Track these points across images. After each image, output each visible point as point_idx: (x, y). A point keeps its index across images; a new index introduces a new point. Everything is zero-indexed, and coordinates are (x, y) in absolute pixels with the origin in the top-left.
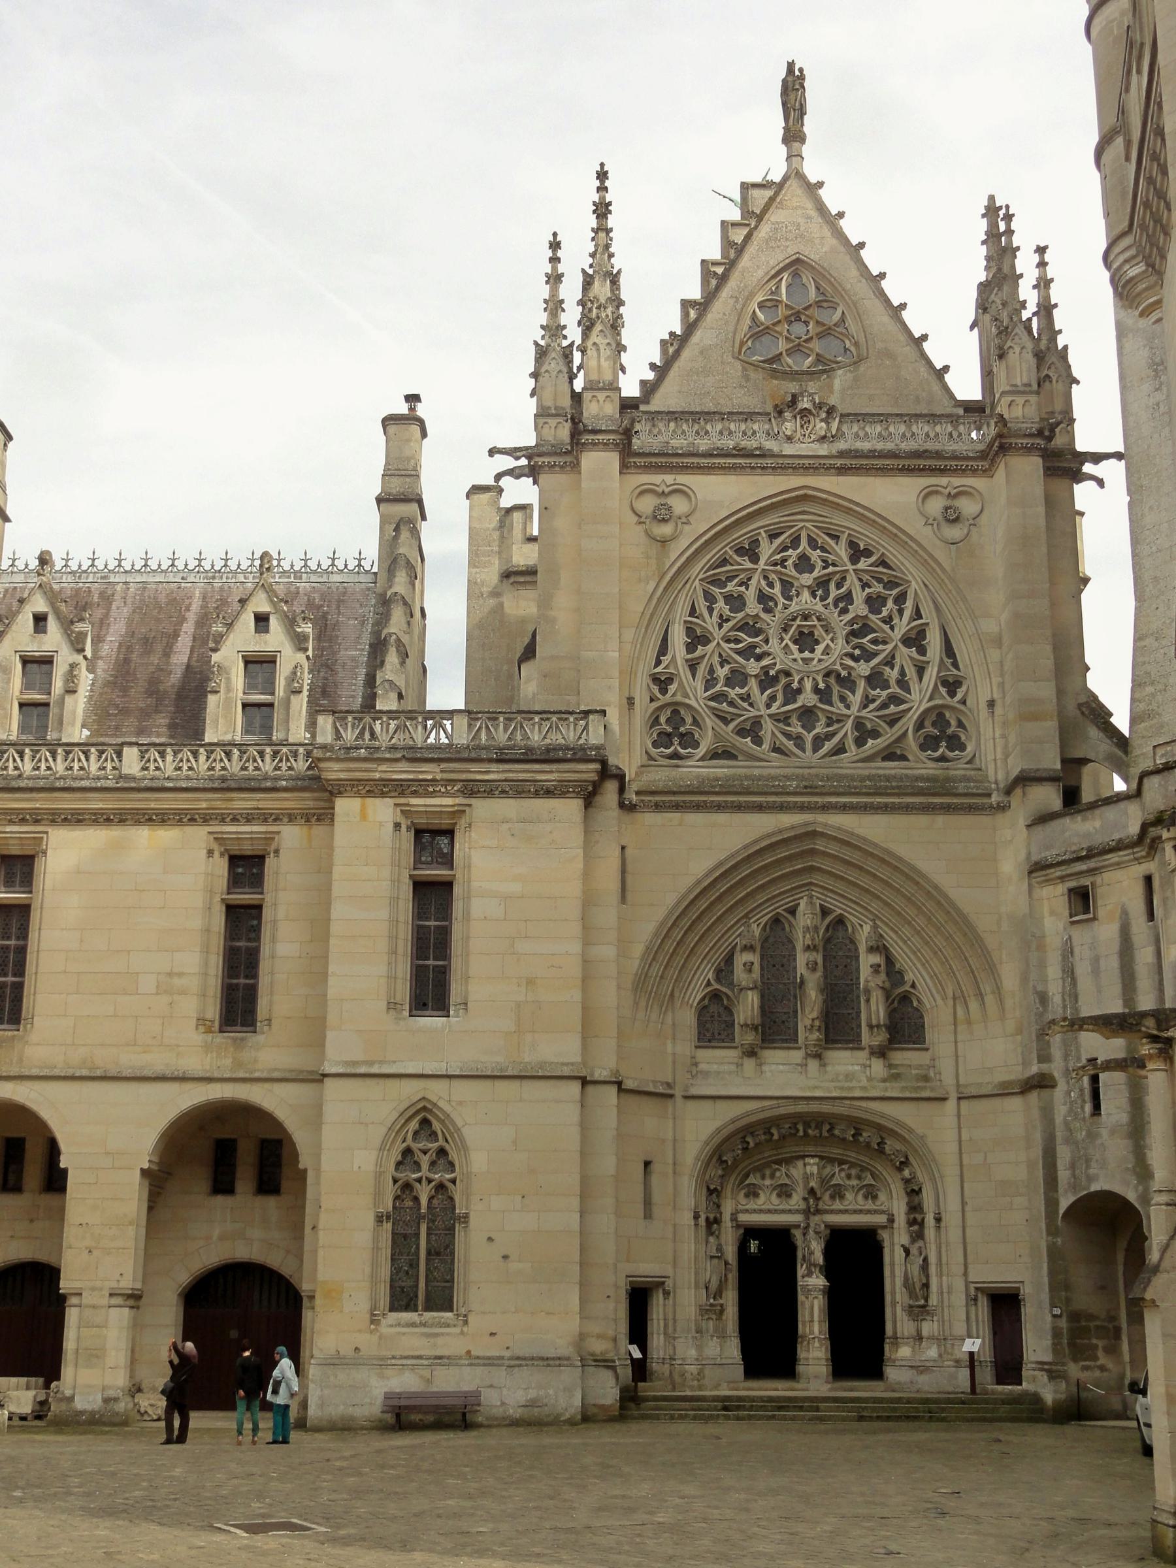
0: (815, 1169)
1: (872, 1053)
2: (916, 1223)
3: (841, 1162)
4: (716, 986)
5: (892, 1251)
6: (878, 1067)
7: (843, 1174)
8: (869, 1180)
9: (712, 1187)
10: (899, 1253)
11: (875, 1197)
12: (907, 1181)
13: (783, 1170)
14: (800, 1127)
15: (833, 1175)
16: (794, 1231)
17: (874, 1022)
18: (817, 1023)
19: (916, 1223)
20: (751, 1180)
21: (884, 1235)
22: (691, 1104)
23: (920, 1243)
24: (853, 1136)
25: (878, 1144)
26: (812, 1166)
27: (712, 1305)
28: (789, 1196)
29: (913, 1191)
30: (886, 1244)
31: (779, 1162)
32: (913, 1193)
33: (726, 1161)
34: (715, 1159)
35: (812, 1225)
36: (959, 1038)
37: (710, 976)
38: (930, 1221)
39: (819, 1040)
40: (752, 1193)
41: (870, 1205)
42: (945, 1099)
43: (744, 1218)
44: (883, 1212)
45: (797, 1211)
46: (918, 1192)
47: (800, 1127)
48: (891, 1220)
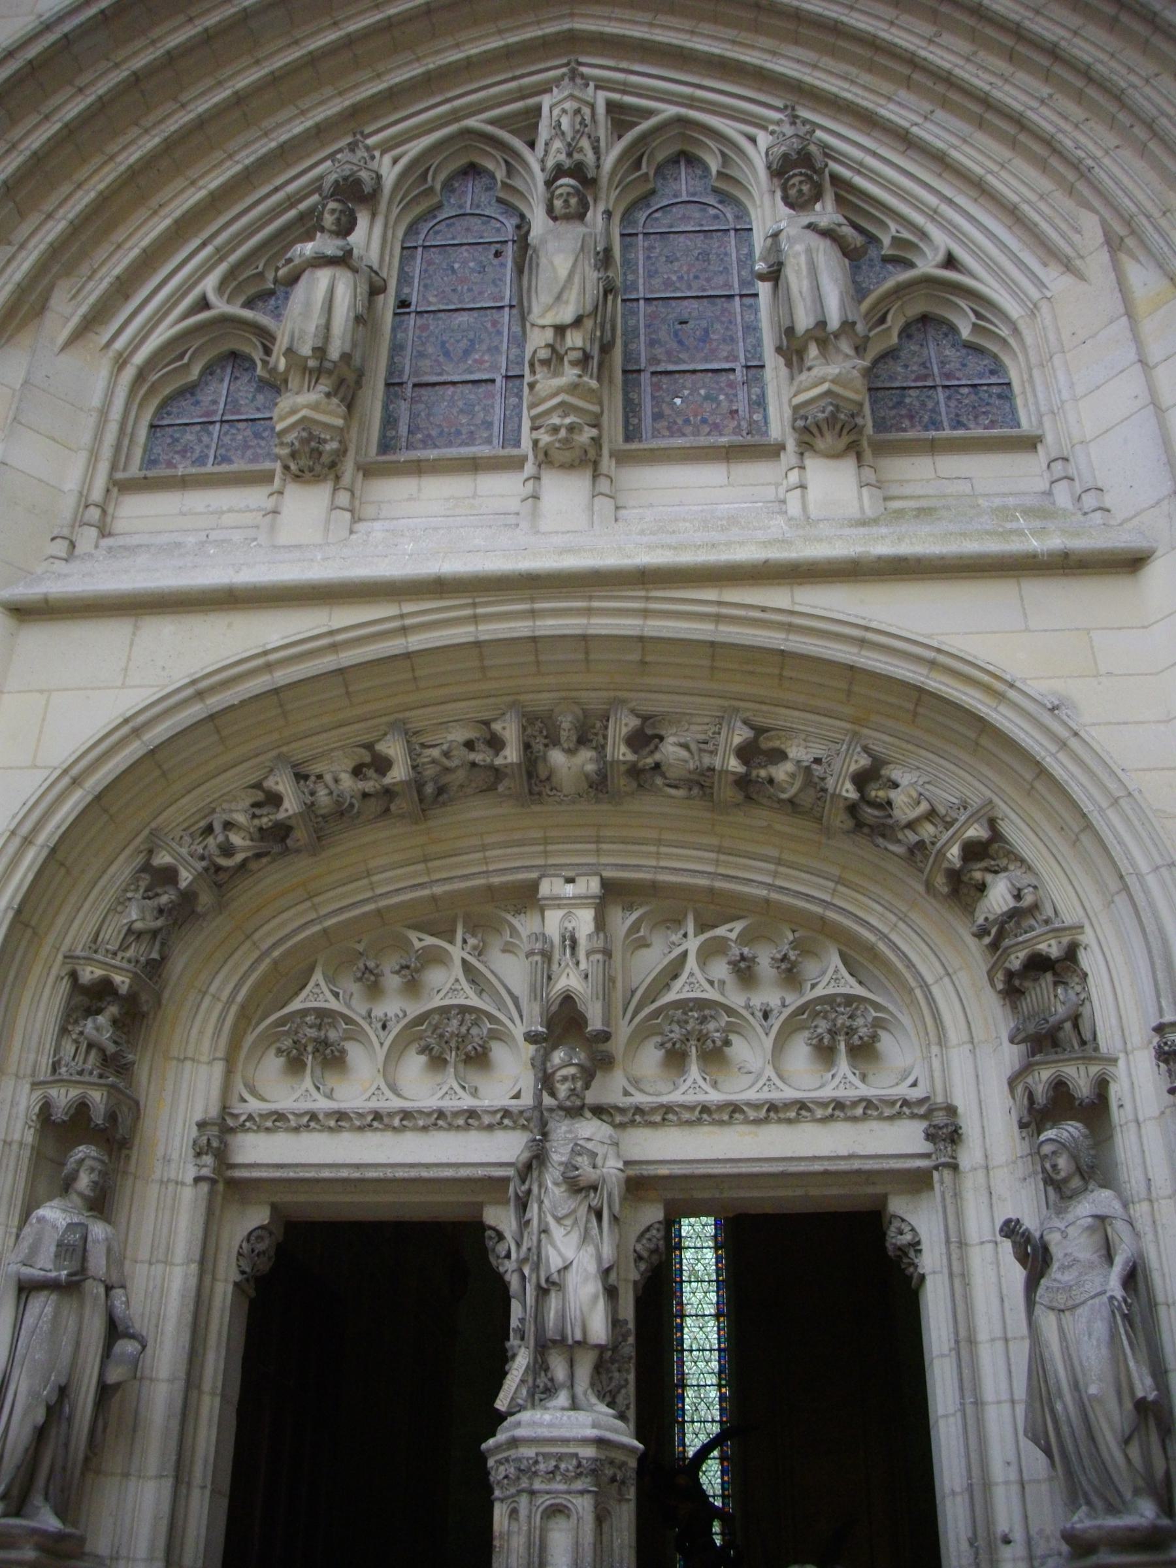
0: (584, 922)
1: (806, 446)
3: (711, 907)
4: (220, 306)
5: (960, 1276)
6: (832, 484)
7: (720, 969)
8: (829, 976)
9: (89, 974)
10: (997, 1273)
11: (864, 1052)
12: (997, 935)
13: (457, 952)
14: (509, 730)
15: (674, 971)
17: (804, 321)
18: (574, 339)
20: (318, 994)
21: (921, 1222)
23: (1098, 1200)
24: (746, 753)
25: (861, 780)
26: (568, 910)
28: (479, 1059)
29: (1038, 964)
31: (440, 918)
32: (1037, 975)
33: (168, 876)
34: (122, 869)
35: (559, 1155)
36: (1155, 352)
37: (209, 284)
39: (573, 388)
40: (318, 1049)
41: (843, 1081)
42: (1131, 563)
43: (258, 1151)
44: (904, 1109)
45: (506, 1118)
46: (1062, 966)
47: (509, 730)
48: (946, 1132)
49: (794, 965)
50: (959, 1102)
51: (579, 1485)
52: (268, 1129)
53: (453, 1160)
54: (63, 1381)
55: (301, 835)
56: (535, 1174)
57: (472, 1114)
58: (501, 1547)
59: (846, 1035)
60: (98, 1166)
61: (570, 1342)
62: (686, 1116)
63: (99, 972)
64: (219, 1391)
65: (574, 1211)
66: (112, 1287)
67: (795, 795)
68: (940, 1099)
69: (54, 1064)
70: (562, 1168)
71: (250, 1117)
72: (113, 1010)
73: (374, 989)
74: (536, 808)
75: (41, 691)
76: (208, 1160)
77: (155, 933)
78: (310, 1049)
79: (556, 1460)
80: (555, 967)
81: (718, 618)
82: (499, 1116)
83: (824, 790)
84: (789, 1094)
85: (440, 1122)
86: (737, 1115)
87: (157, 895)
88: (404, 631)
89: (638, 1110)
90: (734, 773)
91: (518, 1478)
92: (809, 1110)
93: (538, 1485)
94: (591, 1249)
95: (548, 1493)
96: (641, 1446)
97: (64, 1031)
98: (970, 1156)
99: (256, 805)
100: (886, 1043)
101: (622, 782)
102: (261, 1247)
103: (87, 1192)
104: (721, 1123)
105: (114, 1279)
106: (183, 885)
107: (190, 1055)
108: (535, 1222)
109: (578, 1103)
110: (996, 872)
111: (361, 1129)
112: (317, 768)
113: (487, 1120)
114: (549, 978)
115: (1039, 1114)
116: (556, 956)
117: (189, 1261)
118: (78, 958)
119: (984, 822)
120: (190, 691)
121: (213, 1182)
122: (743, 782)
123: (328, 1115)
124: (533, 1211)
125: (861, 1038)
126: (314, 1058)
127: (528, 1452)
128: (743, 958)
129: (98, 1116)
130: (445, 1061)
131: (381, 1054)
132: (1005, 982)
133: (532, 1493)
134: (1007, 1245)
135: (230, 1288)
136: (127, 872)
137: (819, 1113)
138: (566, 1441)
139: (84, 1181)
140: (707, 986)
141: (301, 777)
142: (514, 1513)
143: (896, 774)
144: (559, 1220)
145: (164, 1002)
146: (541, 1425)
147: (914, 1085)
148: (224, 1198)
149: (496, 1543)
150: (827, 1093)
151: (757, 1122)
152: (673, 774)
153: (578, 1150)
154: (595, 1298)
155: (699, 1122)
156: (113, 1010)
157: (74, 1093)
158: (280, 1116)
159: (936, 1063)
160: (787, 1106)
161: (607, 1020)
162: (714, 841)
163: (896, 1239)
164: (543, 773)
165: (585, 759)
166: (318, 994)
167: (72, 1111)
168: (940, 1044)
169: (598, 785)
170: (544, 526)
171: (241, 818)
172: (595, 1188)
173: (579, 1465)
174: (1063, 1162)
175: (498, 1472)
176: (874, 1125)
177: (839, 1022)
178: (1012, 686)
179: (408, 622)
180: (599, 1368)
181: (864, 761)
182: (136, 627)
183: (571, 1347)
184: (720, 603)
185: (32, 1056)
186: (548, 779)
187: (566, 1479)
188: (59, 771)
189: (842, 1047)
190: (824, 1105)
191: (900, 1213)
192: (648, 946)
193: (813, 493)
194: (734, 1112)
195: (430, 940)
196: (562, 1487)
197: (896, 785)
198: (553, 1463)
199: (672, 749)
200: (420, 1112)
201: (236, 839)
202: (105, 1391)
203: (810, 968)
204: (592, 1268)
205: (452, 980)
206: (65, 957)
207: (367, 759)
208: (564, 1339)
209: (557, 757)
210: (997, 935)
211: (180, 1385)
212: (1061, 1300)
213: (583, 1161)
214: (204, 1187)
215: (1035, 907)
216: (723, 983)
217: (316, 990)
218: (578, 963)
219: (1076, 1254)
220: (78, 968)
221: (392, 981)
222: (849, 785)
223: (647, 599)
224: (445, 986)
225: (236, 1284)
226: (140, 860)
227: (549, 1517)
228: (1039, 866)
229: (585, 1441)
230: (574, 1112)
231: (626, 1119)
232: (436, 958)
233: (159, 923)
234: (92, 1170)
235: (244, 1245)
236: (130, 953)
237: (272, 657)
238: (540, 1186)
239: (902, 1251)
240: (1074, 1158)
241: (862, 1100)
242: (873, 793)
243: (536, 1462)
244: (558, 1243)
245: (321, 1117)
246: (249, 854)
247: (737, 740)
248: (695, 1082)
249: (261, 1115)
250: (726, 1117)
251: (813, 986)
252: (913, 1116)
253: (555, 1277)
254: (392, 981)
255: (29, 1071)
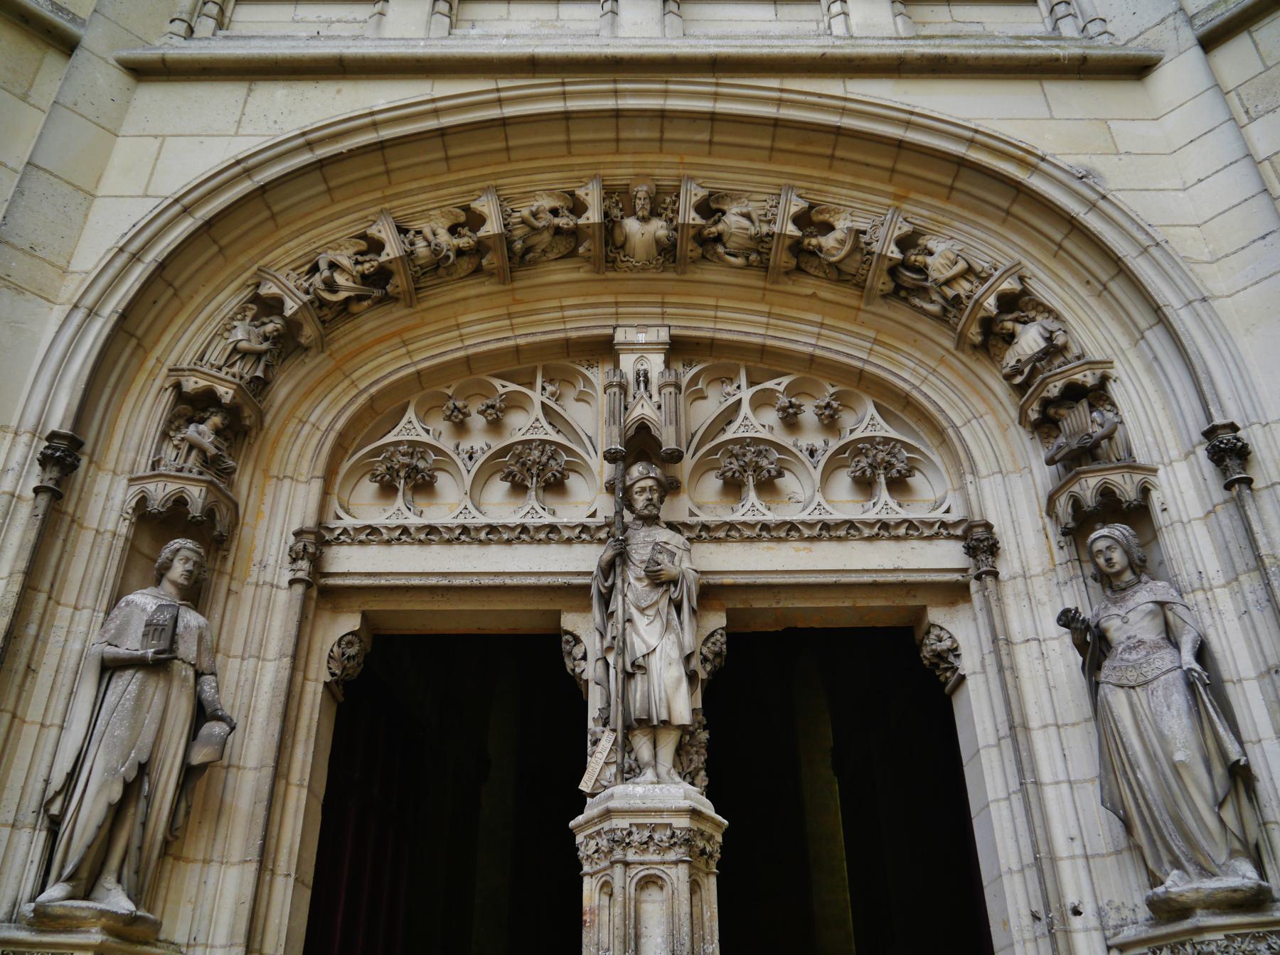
2: (1106, 521)
7: (771, 416)
9: (192, 384)
11: (899, 485)
13: (536, 396)
14: (592, 196)
16: (570, 621)
19: (1106, 521)
20: (410, 428)
21: (959, 629)
22: (154, 96)
24: (801, 220)
27: (44, 919)
28: (556, 486)
29: (1074, 393)
30: (972, 660)
31: (523, 364)
32: (1066, 409)
34: (230, 299)
35: (640, 550)
38: (1182, 489)
41: (884, 506)
44: (943, 530)
45: (584, 533)
49: (836, 411)
50: (992, 521)
51: (671, 856)
52: (361, 542)
53: (535, 570)
54: (144, 759)
55: (399, 283)
56: (618, 570)
57: (553, 528)
58: (592, 921)
59: (882, 470)
60: (195, 557)
61: (655, 722)
62: (747, 533)
63: (203, 383)
64: (306, 783)
65: (657, 602)
66: (203, 674)
67: (841, 261)
68: (977, 518)
69: (153, 463)
70: (644, 566)
71: (345, 531)
72: (216, 420)
73: (461, 427)
74: (611, 275)
75: (156, 137)
76: (304, 564)
77: (258, 355)
78: (402, 474)
79: (648, 831)
80: (630, 399)
81: (780, 102)
82: (577, 530)
83: (870, 253)
84: (838, 516)
85: (523, 536)
86: (793, 533)
87: (264, 324)
88: (500, 102)
89: (705, 527)
90: (791, 237)
91: (611, 851)
92: (857, 529)
93: (631, 857)
94: (673, 637)
95: (641, 864)
96: (726, 822)
97: (165, 436)
98: (1007, 565)
99: (361, 253)
100: (916, 481)
101: (690, 247)
102: (352, 651)
103: (181, 580)
104: (779, 539)
105: (205, 664)
106: (288, 313)
107: (289, 472)
108: (620, 611)
109: (655, 512)
110: (1025, 323)
111: (449, 542)
112: (417, 225)
113: (566, 534)
114: (626, 408)
115: (1077, 527)
116: (632, 389)
117: (282, 656)
118: (183, 370)
119: (1016, 277)
120: (301, 141)
121: (309, 585)
122: (797, 248)
123: (419, 529)
124: (617, 604)
125: (899, 472)
126: (406, 483)
127: (622, 823)
128: (791, 405)
129: (195, 509)
130: (527, 487)
131: (468, 479)
132: (1039, 412)
133: (627, 864)
134: (1066, 636)
135: (320, 688)
136: (234, 303)
137: (867, 532)
138: (659, 812)
139: (178, 571)
140: (760, 428)
141: (402, 230)
142: (606, 887)
143: (932, 244)
144: (642, 611)
145: (266, 424)
146: (634, 796)
147: (948, 511)
148: (317, 607)
149: (586, 917)
150: (871, 516)
151: (811, 539)
152: (732, 245)
153: (659, 547)
154: (679, 681)
155: (758, 538)
156: (216, 420)
157: (172, 487)
158: (373, 530)
159: (971, 489)
160: (839, 525)
161: (678, 442)
162: (765, 308)
163: (932, 644)
164: (619, 239)
165: (658, 228)
166: (410, 428)
167: (169, 504)
168: (973, 473)
169: (667, 251)
170: (621, 33)
171: (345, 262)
172: (674, 582)
173: (673, 835)
174: (1118, 557)
175: (585, 844)
176: (915, 543)
177: (880, 456)
178: (1043, 159)
179: (503, 94)
180: (680, 750)
181: (907, 228)
182: (250, 90)
183: (654, 727)
184: (782, 90)
185: (131, 455)
186: (623, 247)
187: (661, 850)
188: (170, 201)
189: (882, 479)
190: (871, 525)
191: (939, 622)
192: (705, 398)
193: (854, 19)
194: (789, 530)
195: (512, 387)
196: (656, 858)
197: (931, 253)
198: (647, 833)
199: (734, 218)
200: (505, 526)
201: (340, 279)
202: (189, 773)
203: (847, 419)
204: (675, 654)
205: (533, 419)
206: (170, 370)
207: (462, 219)
208: (650, 719)
209: (632, 225)
210: (1023, 382)
211: (268, 772)
212: (1132, 677)
213: (663, 558)
214: (299, 589)
215: (1064, 348)
216: (771, 428)
217: (408, 426)
218: (651, 397)
219: (1139, 637)
220: (183, 379)
221: (477, 422)
222: (893, 247)
223: (717, 85)
224: (524, 425)
225: (326, 683)
226: (247, 293)
227: (642, 889)
228: (1066, 314)
229: (678, 812)
230: (651, 520)
231: (693, 535)
232: (515, 403)
233: (265, 346)
234: (187, 560)
235: (335, 649)
236: (236, 369)
237: (379, 117)
238: (623, 581)
239: (940, 656)
240: (1127, 552)
241: (905, 521)
242: (913, 258)
243: (630, 833)
244: (642, 632)
245: (412, 530)
246: (352, 294)
247: (794, 209)
248: (753, 505)
249: (355, 529)
250: (783, 535)
251: (852, 431)
252: (950, 537)
253: (641, 661)
254: (477, 422)
255: (127, 468)
